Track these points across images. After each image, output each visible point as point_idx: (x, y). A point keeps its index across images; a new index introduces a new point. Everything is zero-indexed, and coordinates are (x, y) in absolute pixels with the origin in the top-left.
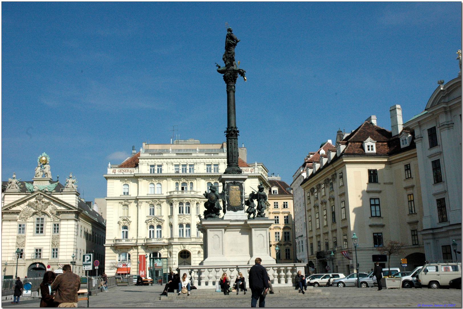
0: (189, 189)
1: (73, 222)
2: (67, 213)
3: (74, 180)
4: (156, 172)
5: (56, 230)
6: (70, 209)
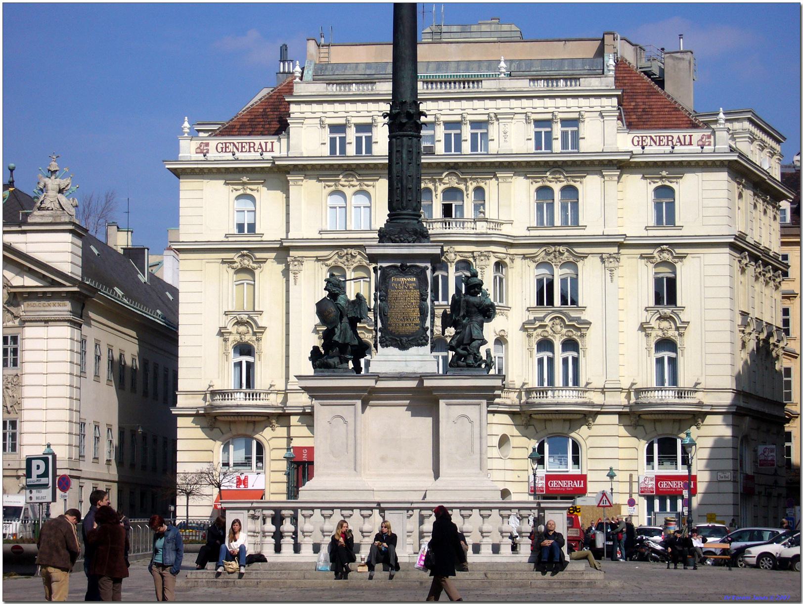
0: (469, 211)
1: (65, 331)
2: (45, 296)
3: (63, 183)
4: (351, 150)
5: (10, 357)
6: (54, 283)
